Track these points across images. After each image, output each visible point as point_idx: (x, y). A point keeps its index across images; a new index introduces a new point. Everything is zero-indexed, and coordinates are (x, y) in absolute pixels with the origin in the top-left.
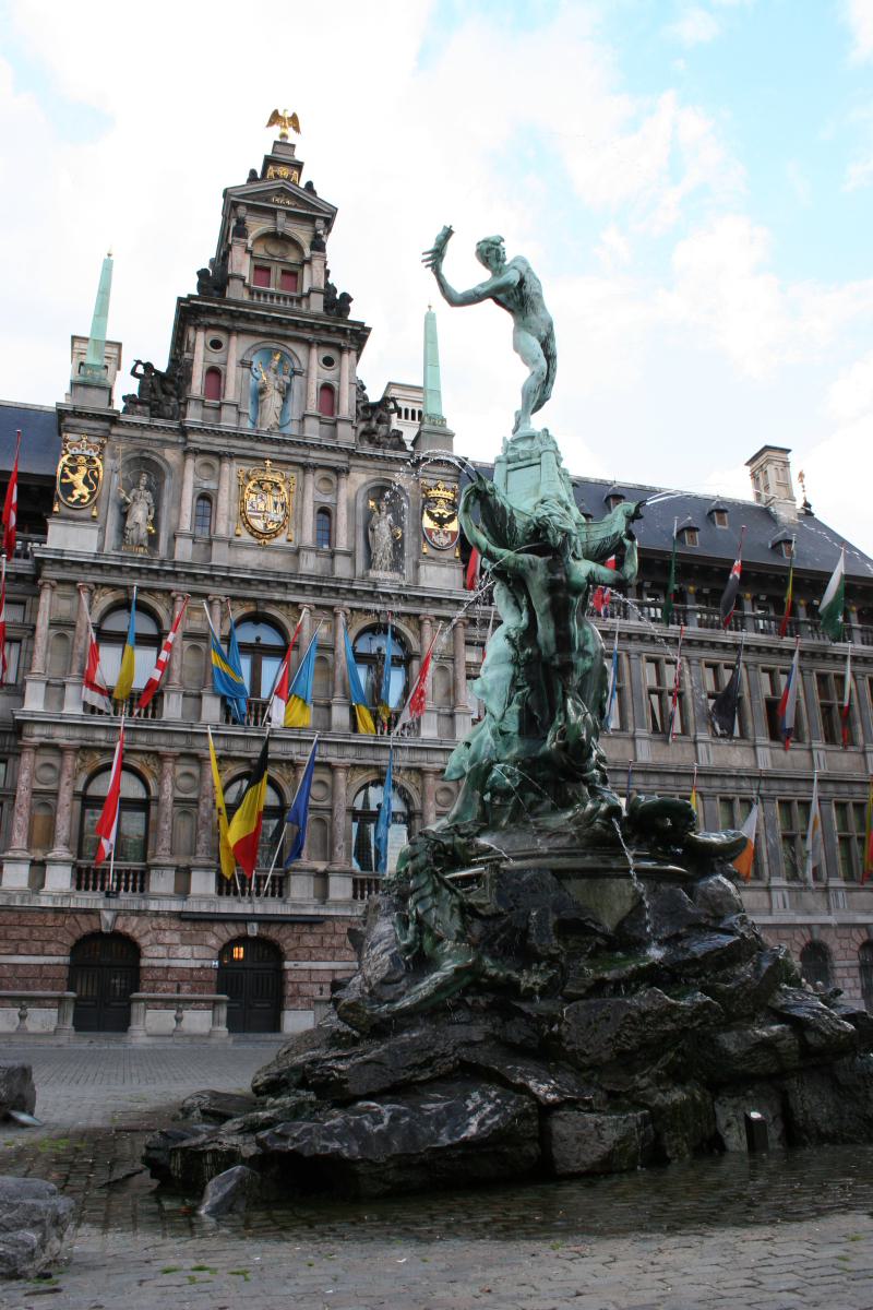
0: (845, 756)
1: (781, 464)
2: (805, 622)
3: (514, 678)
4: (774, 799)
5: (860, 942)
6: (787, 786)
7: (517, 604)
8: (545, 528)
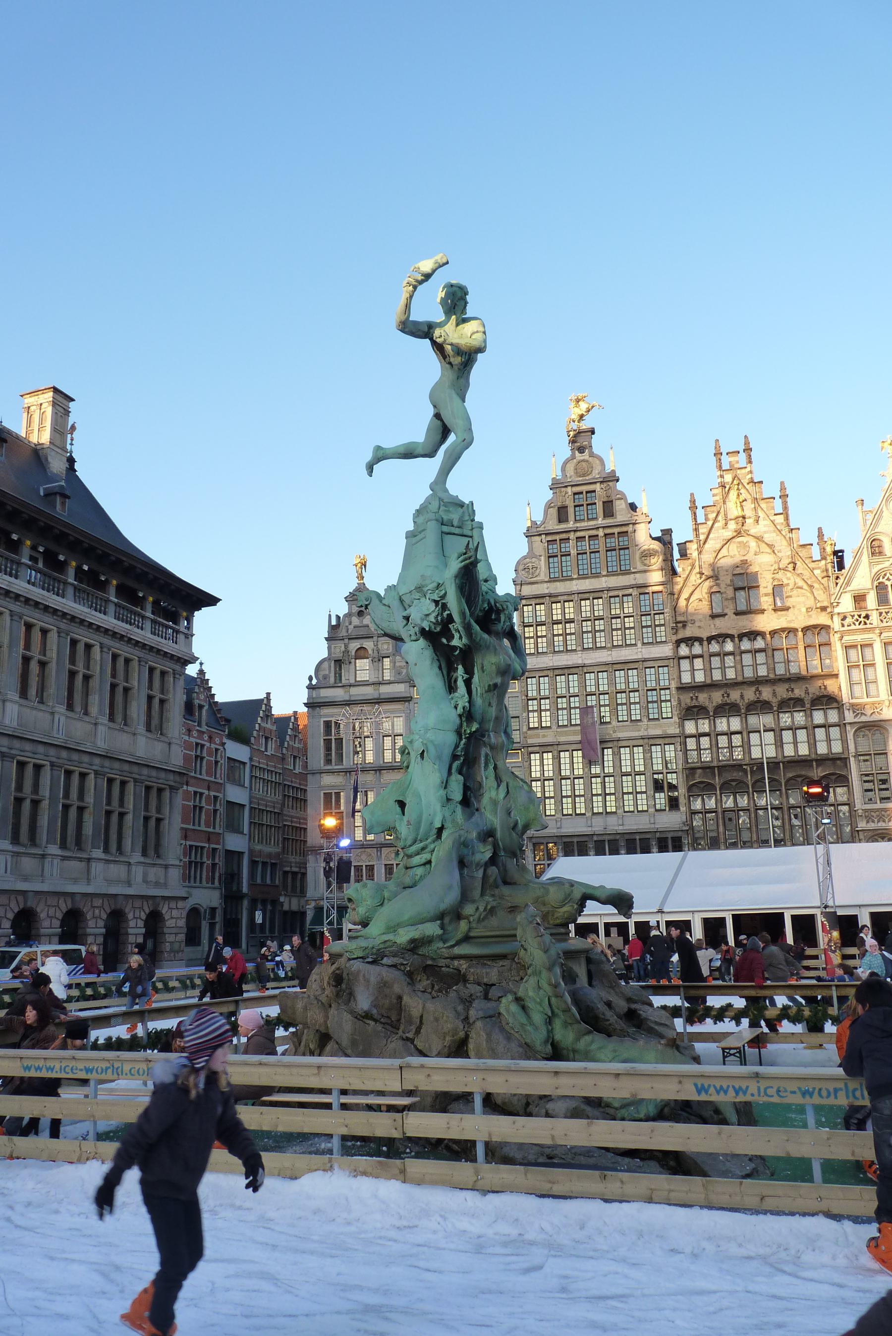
0: (79, 725)
1: (62, 410)
2: (72, 584)
3: (457, 746)
4: (13, 758)
5: (65, 910)
6: (28, 747)
7: (440, 668)
8: (498, 612)
